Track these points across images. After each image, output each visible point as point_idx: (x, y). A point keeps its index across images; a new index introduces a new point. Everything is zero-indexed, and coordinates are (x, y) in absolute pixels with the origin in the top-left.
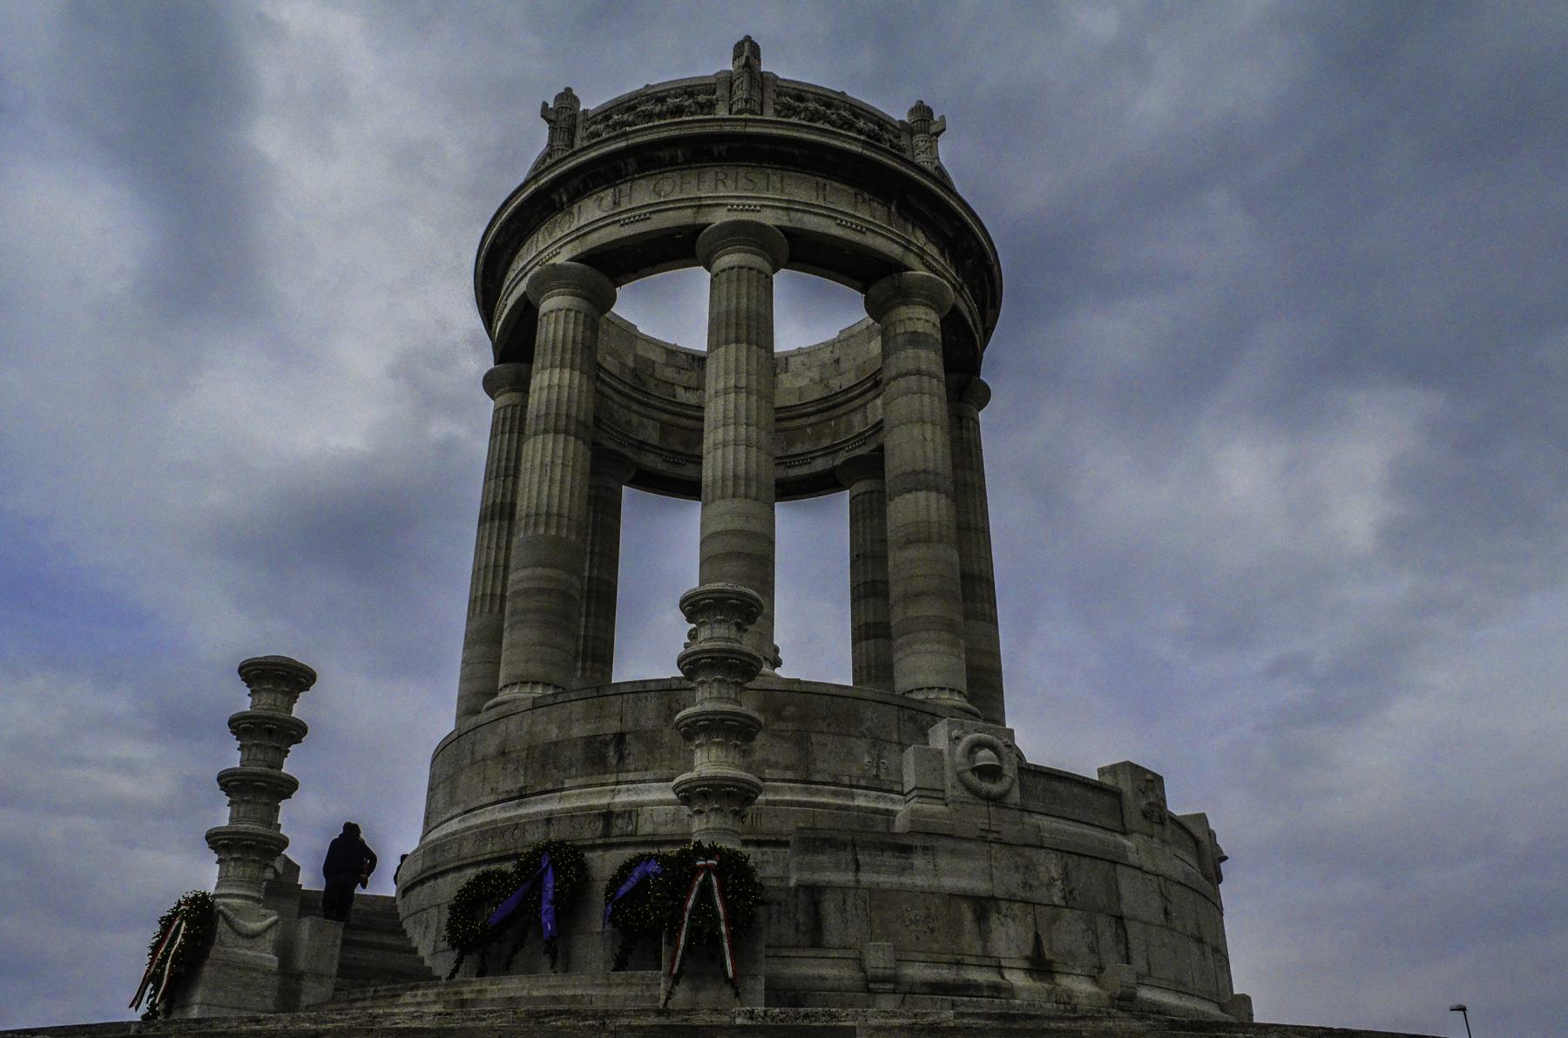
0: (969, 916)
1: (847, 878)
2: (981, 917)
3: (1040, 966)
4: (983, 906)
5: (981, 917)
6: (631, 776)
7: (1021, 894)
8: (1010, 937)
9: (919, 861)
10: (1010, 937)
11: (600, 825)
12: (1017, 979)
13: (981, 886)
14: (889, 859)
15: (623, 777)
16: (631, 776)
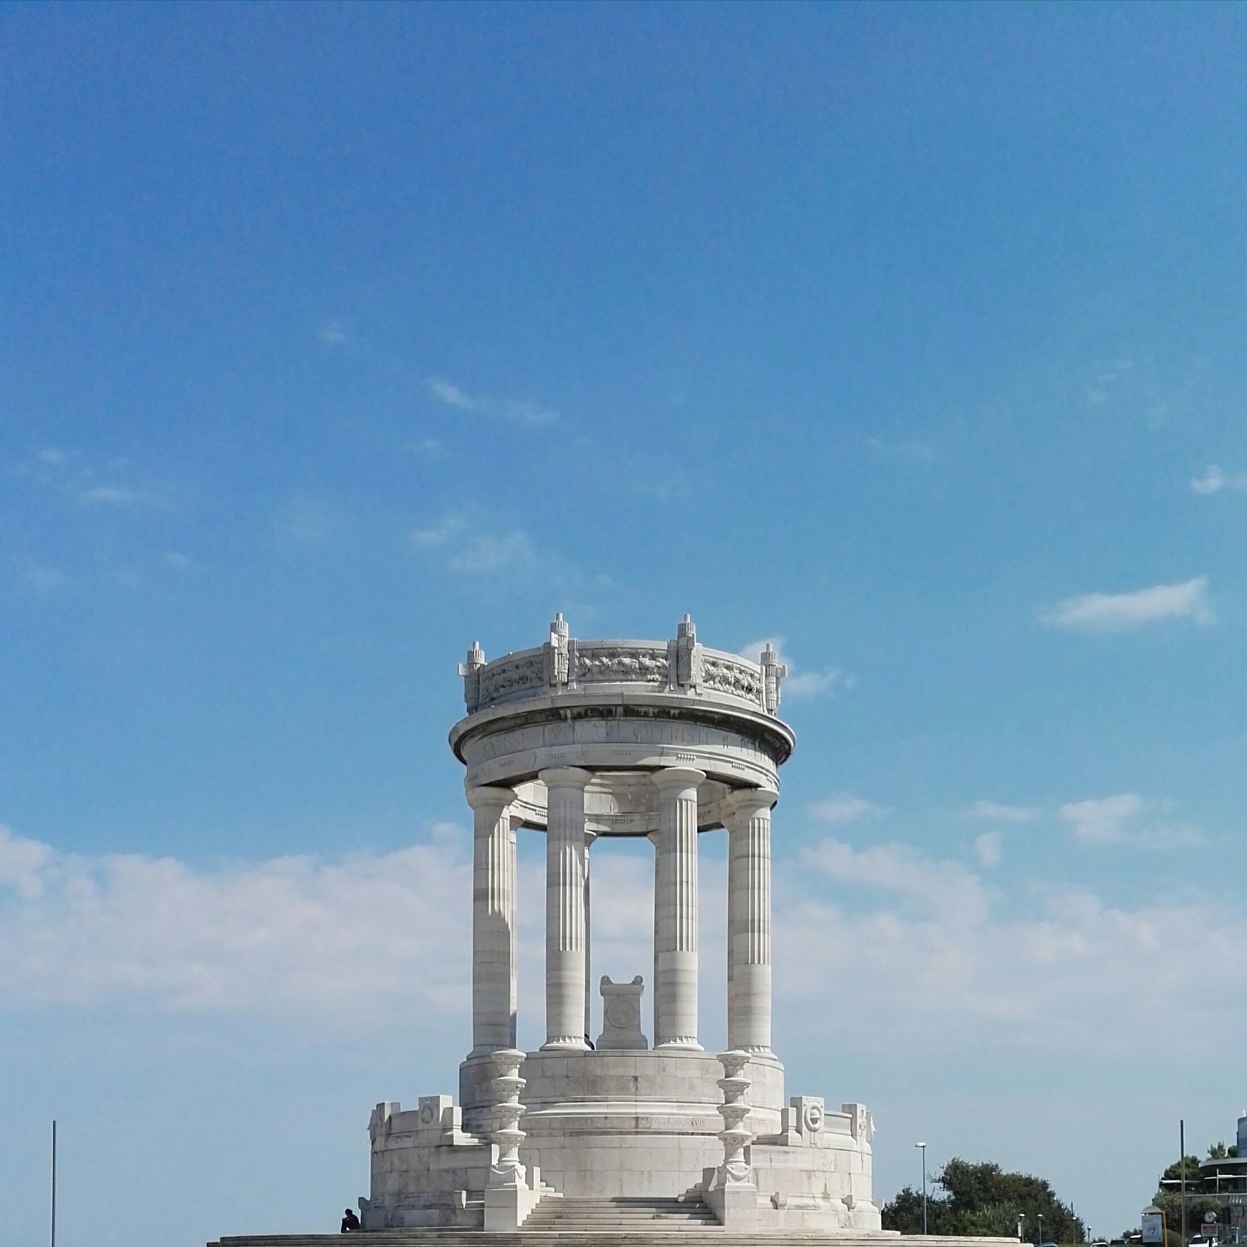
0: (806, 1178)
1: (767, 1165)
2: (809, 1178)
3: (826, 1197)
4: (810, 1173)
5: (809, 1178)
6: (643, 1098)
7: (822, 1168)
8: (817, 1188)
9: (791, 1156)
10: (817, 1186)
11: (633, 1123)
12: (820, 1202)
13: (810, 1167)
14: (782, 1157)
15: (638, 1098)
16: (643, 1098)
